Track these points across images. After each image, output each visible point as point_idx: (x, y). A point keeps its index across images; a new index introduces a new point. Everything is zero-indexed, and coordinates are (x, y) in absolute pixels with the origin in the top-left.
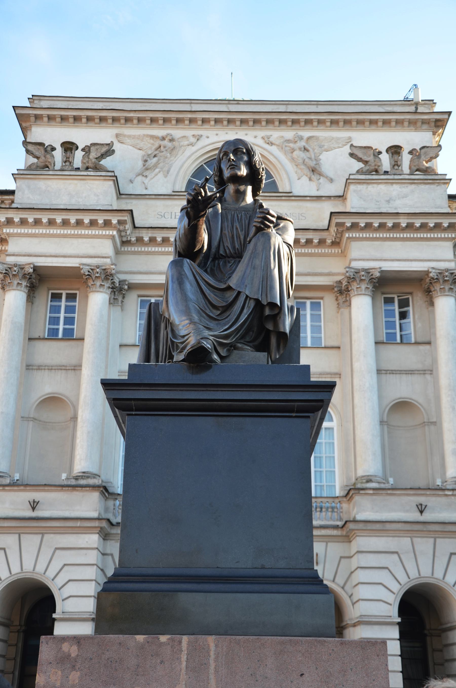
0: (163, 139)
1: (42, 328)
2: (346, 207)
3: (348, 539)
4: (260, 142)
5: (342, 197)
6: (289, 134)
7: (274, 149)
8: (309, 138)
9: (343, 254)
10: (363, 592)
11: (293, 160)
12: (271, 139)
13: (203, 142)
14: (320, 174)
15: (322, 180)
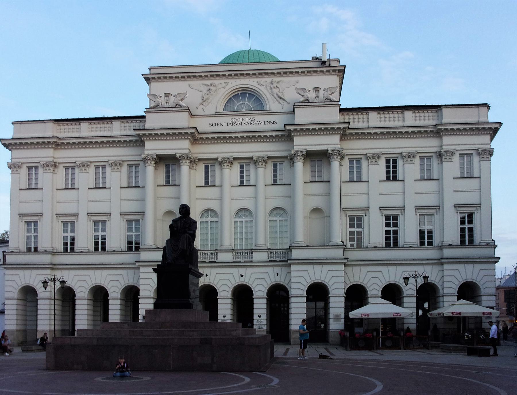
0: (211, 85)
1: (163, 181)
2: (294, 118)
3: (290, 265)
4: (256, 84)
5: (293, 112)
6: (269, 80)
7: (262, 88)
8: (278, 82)
9: (292, 140)
10: (293, 286)
11: (272, 94)
12: (262, 83)
13: (230, 86)
14: (284, 100)
15: (285, 103)
